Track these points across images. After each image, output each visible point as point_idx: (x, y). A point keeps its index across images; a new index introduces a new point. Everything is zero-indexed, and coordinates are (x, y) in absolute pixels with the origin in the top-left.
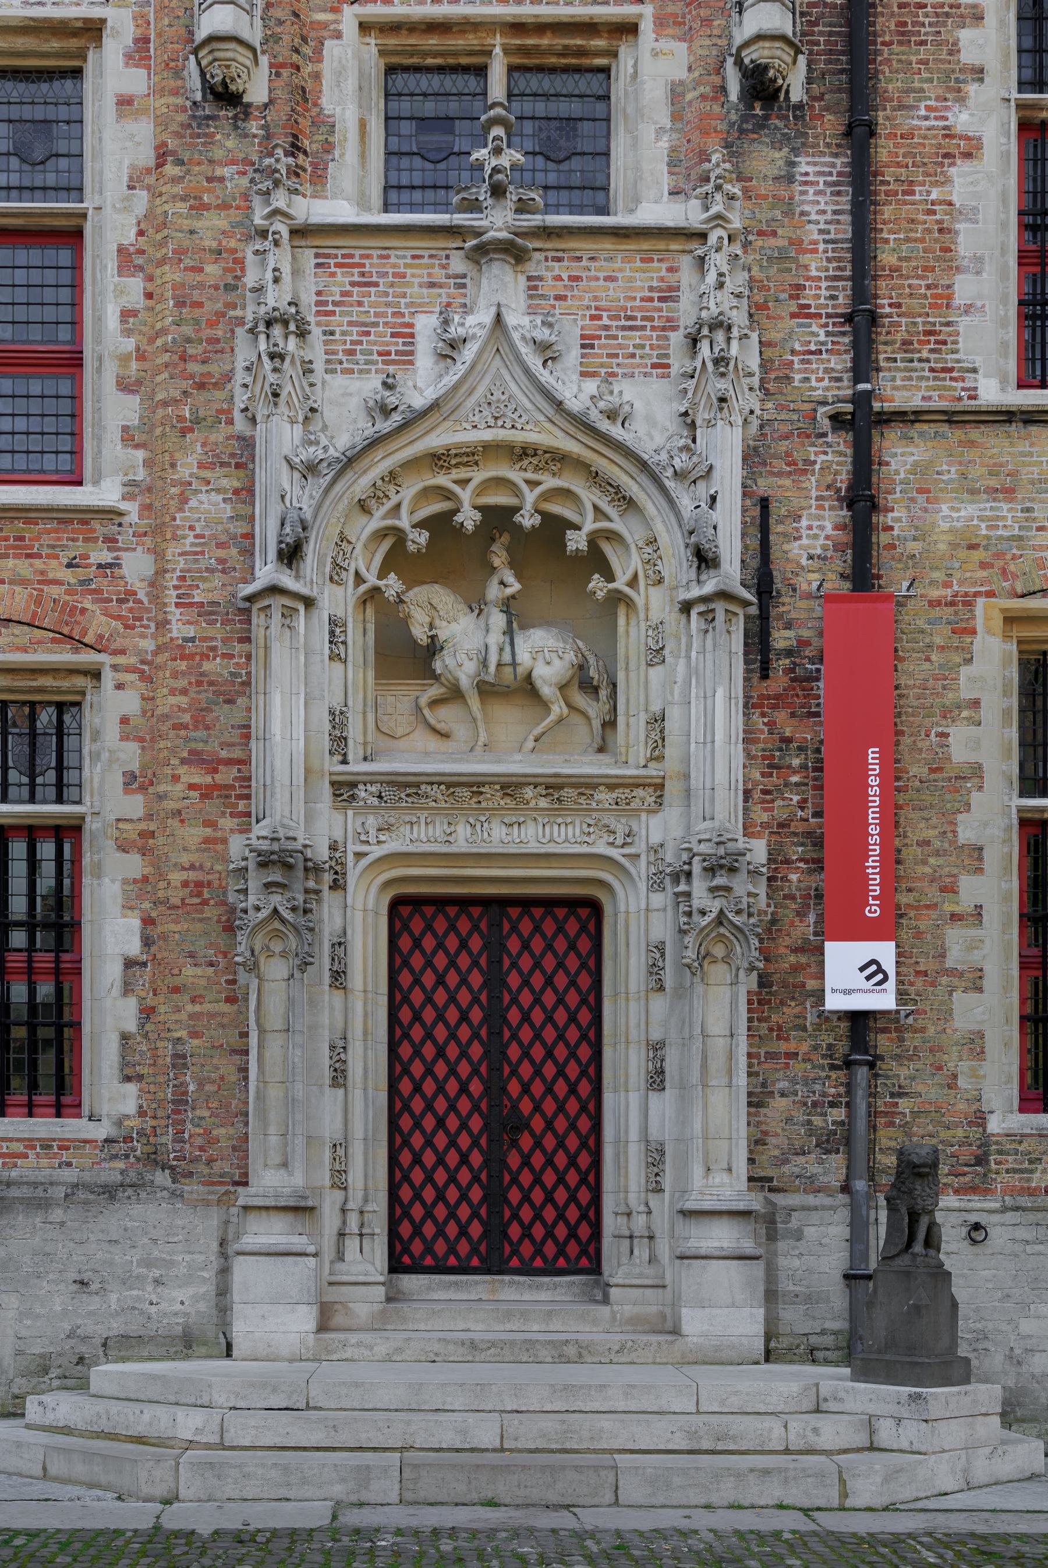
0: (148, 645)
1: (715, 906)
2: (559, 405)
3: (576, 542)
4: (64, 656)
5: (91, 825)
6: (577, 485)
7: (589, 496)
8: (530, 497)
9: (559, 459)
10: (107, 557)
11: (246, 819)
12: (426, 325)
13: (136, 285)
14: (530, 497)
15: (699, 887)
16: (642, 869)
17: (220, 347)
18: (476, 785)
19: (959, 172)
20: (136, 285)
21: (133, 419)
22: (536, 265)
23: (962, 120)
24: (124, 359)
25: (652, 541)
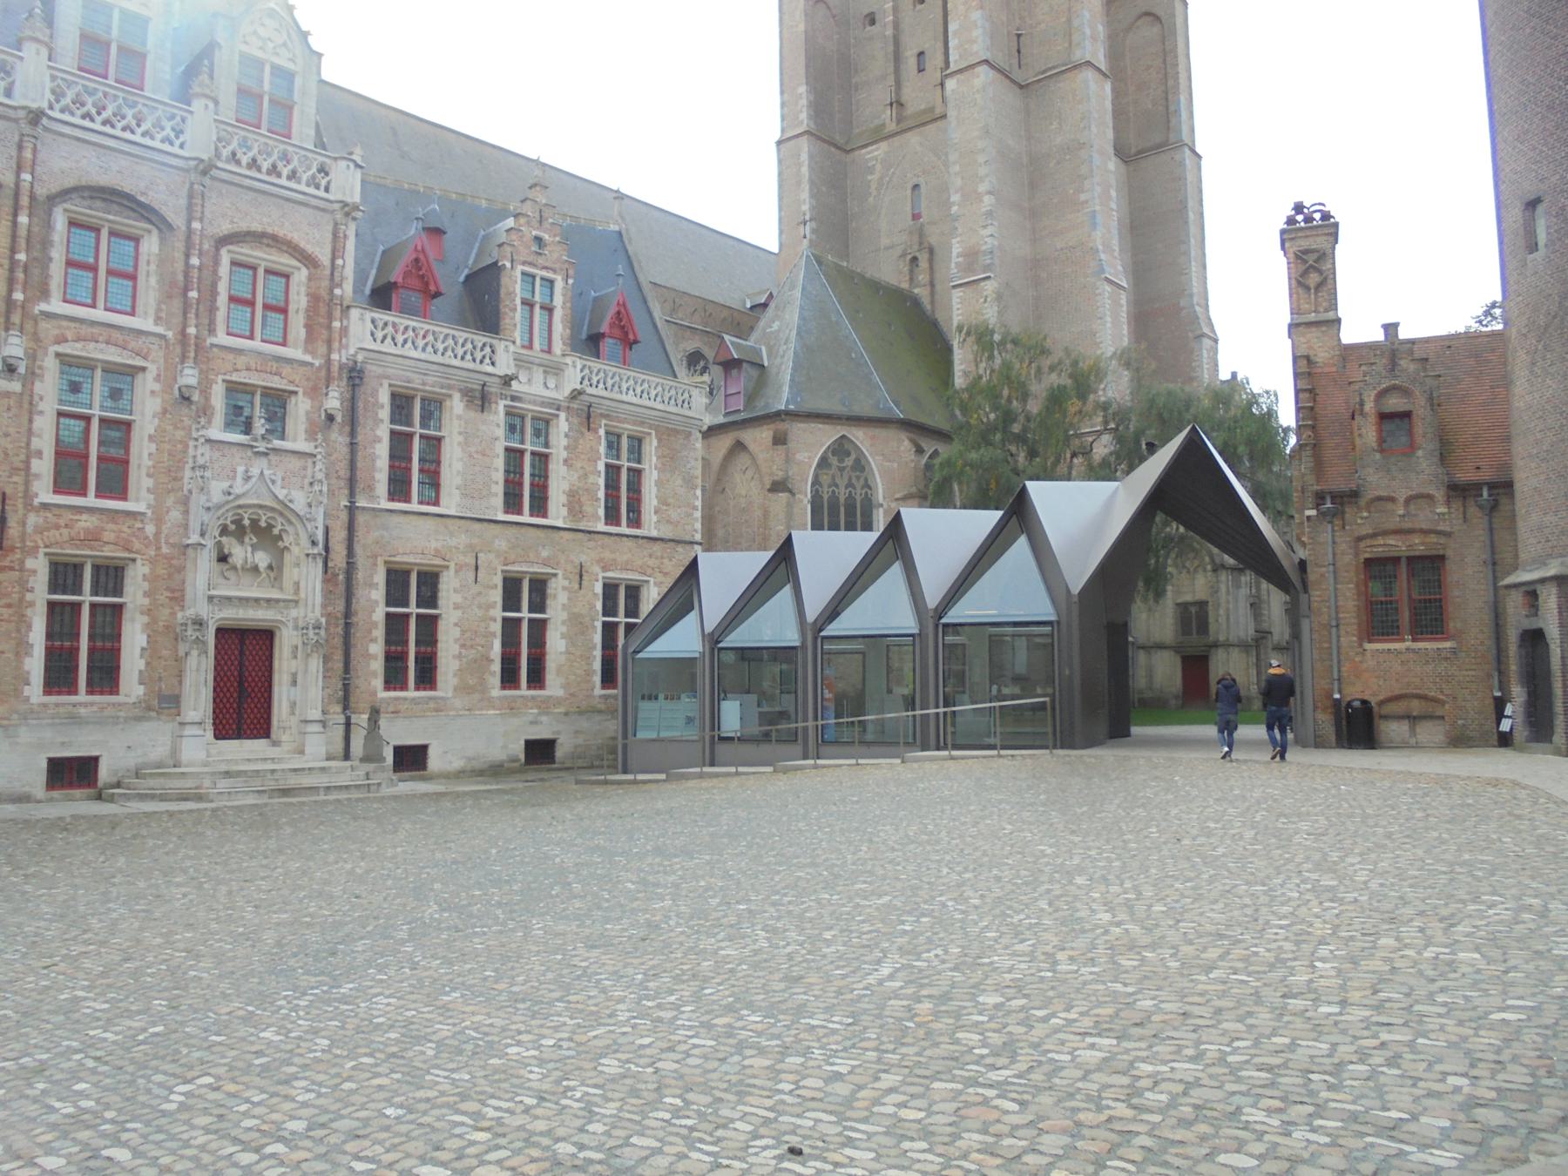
0: (153, 553)
1: (316, 638)
2: (276, 497)
3: (276, 531)
4: (126, 555)
5: (130, 606)
6: (277, 516)
7: (280, 519)
8: (264, 518)
9: (272, 509)
10: (140, 526)
11: (183, 608)
12: (240, 469)
13: (153, 447)
14: (264, 518)
15: (311, 633)
16: (291, 624)
18: (247, 599)
19: (378, 446)
20: (153, 447)
21: (151, 486)
22: (271, 457)
23: (379, 433)
24: (149, 468)
25: (297, 534)
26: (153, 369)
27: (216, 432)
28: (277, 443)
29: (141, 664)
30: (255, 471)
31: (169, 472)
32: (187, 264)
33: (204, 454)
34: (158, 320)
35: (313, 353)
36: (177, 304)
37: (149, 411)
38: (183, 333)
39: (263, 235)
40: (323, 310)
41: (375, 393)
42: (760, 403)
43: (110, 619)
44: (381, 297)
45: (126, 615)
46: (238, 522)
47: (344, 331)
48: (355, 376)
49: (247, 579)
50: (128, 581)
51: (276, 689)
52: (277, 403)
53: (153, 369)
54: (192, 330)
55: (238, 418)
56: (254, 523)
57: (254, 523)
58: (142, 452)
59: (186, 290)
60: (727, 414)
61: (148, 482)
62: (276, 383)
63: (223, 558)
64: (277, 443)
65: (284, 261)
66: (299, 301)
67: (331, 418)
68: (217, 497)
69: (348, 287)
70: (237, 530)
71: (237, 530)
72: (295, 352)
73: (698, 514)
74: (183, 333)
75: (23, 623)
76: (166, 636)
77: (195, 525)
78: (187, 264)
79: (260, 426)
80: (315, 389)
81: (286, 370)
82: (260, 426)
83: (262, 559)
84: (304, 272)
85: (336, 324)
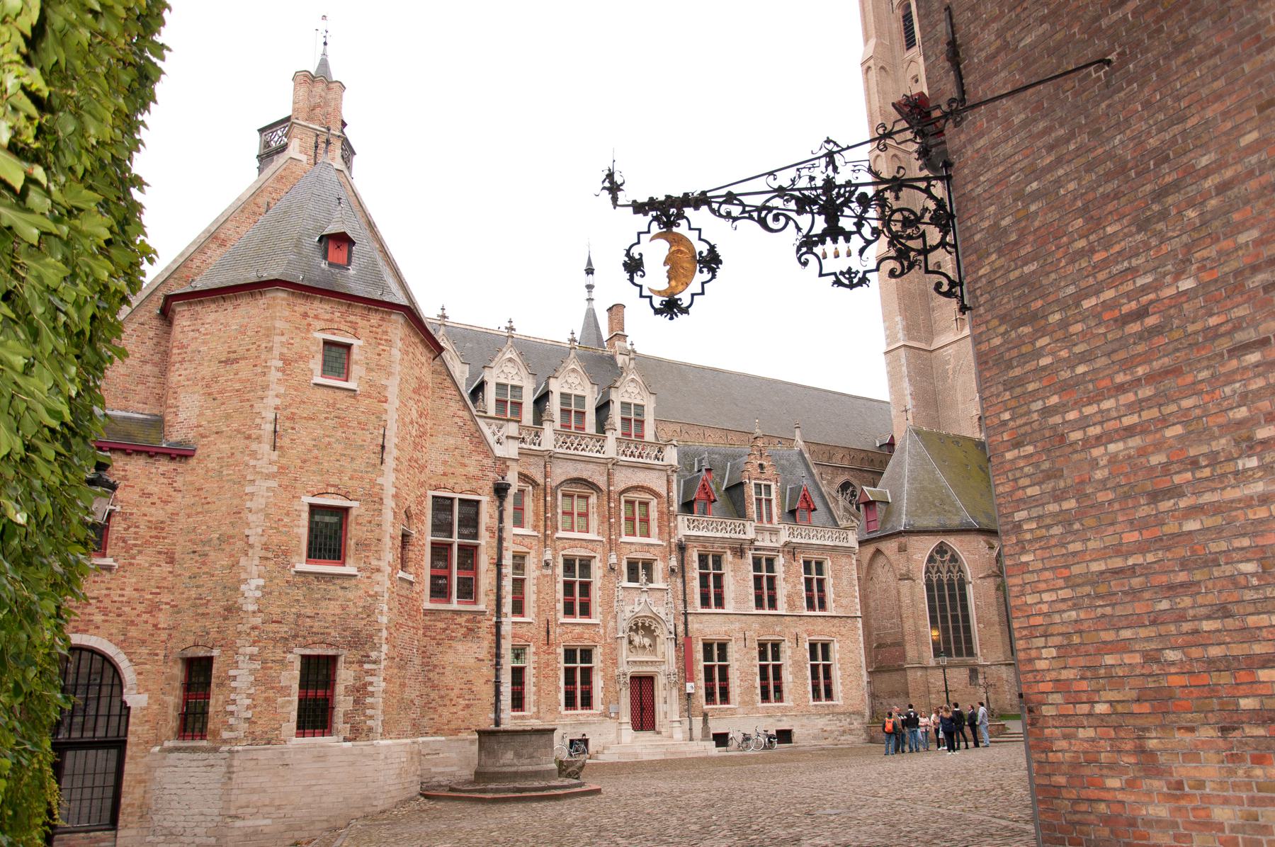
11: (617, 668)
12: (636, 600)
17: (612, 602)
26: (598, 557)
27: (626, 584)
28: (651, 586)
29: (601, 695)
30: (643, 600)
31: (608, 604)
32: (610, 507)
33: (621, 594)
34: (599, 533)
35: (662, 540)
36: (606, 526)
37: (598, 577)
38: (610, 539)
39: (638, 487)
40: (665, 518)
41: (691, 556)
42: (889, 526)
43: (587, 673)
44: (687, 507)
45: (594, 673)
46: (636, 625)
47: (676, 526)
48: (682, 548)
49: (640, 651)
50: (594, 657)
51: (657, 706)
52: (648, 565)
53: (598, 557)
54: (613, 537)
55: (633, 576)
56: (643, 624)
57: (643, 624)
58: (596, 595)
59: (610, 518)
60: (869, 533)
61: (599, 609)
62: (648, 556)
63: (631, 642)
64: (651, 586)
65: (645, 496)
66: (654, 515)
67: (673, 570)
68: (628, 615)
69: (675, 507)
70: (635, 628)
71: (635, 628)
72: (653, 540)
73: (857, 600)
74: (610, 539)
75: (557, 677)
76: (611, 680)
77: (620, 628)
78: (610, 507)
79: (643, 578)
80: (665, 557)
81: (652, 549)
82: (643, 578)
83: (647, 641)
84: (655, 500)
85: (672, 524)
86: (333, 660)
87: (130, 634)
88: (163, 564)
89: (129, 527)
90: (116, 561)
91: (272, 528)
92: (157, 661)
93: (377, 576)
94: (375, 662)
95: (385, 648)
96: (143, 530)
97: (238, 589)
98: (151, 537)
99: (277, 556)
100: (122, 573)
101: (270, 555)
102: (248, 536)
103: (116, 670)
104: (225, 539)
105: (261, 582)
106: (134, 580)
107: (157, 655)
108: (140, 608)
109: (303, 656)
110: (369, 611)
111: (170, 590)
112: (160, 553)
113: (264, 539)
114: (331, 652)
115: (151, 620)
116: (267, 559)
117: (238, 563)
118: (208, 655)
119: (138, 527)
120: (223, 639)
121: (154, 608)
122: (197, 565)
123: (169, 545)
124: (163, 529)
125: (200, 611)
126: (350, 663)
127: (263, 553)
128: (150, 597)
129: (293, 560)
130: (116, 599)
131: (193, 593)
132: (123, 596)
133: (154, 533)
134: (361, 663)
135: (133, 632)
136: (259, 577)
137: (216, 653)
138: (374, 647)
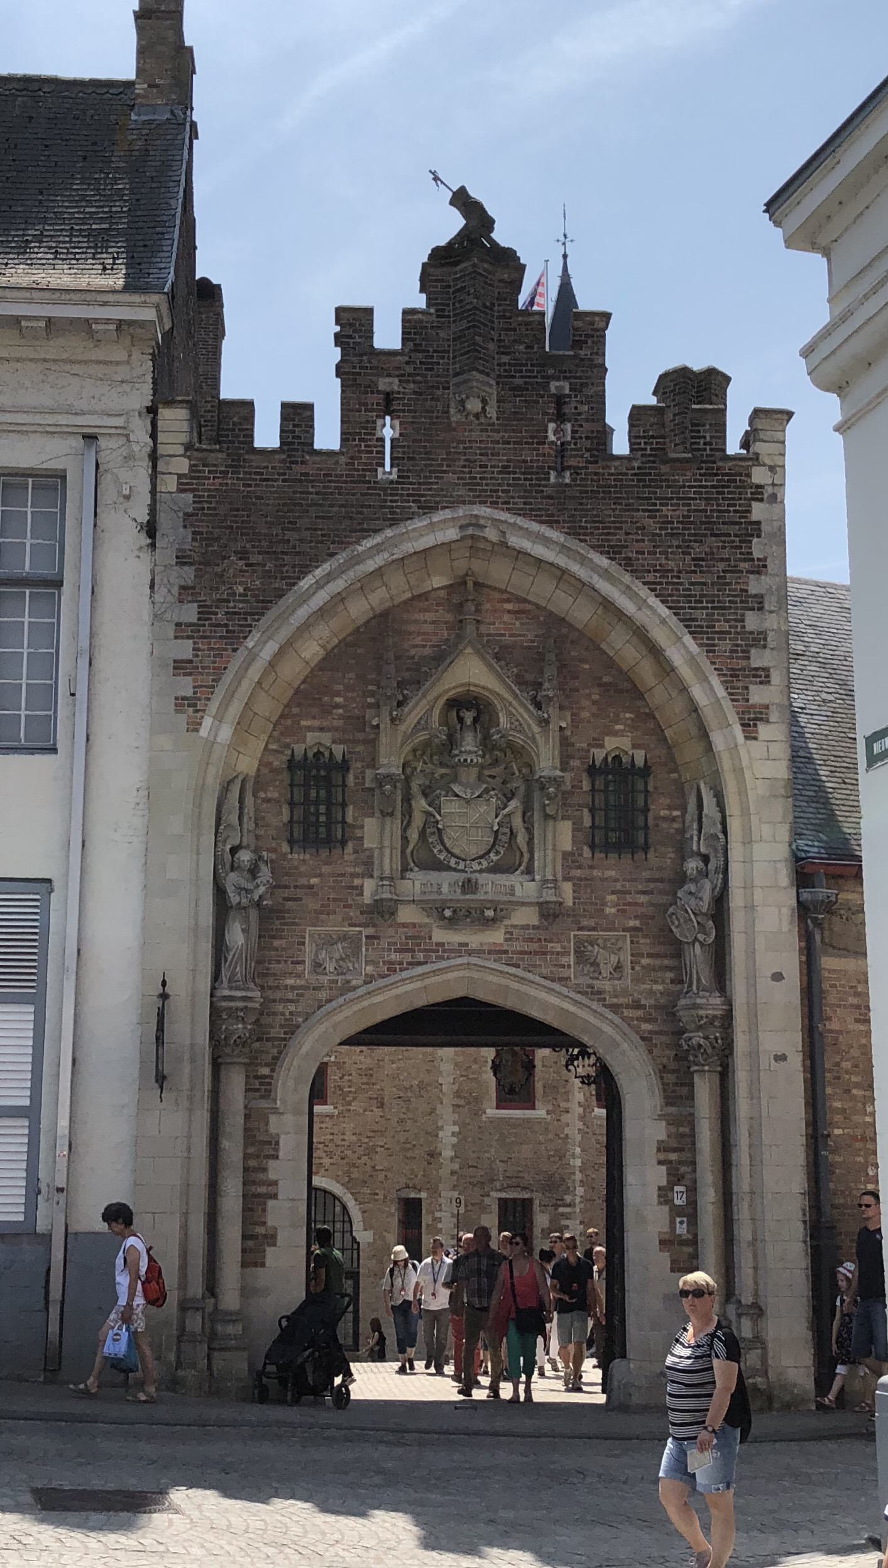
86: (530, 1201)
87: (353, 1176)
88: (375, 1109)
89: (343, 1076)
90: (335, 1108)
91: (462, 1076)
92: (377, 1200)
93: (565, 1118)
94: (569, 1205)
95: (580, 1191)
96: (355, 1077)
97: (437, 1136)
98: (362, 1084)
99: (469, 1103)
100: (341, 1119)
101: (462, 1102)
102: (441, 1085)
103: (344, 1208)
104: (422, 1086)
105: (456, 1129)
106: (352, 1125)
107: (377, 1194)
108: (360, 1151)
109: (500, 1199)
110: (561, 1155)
111: (382, 1133)
112: (370, 1098)
113: (456, 1087)
114: (526, 1195)
115: (369, 1163)
116: (458, 1106)
117: (435, 1109)
118: (418, 1196)
119: (351, 1075)
120: (429, 1182)
121: (370, 1151)
122: (404, 1110)
123: (379, 1090)
124: (371, 1075)
125: (409, 1154)
126: (545, 1206)
127: (457, 1101)
128: (366, 1140)
129: (484, 1106)
130: (339, 1143)
131: (402, 1137)
132: (344, 1140)
133: (365, 1080)
134: (556, 1206)
135: (355, 1175)
136: (454, 1125)
137: (423, 1195)
138: (567, 1191)
